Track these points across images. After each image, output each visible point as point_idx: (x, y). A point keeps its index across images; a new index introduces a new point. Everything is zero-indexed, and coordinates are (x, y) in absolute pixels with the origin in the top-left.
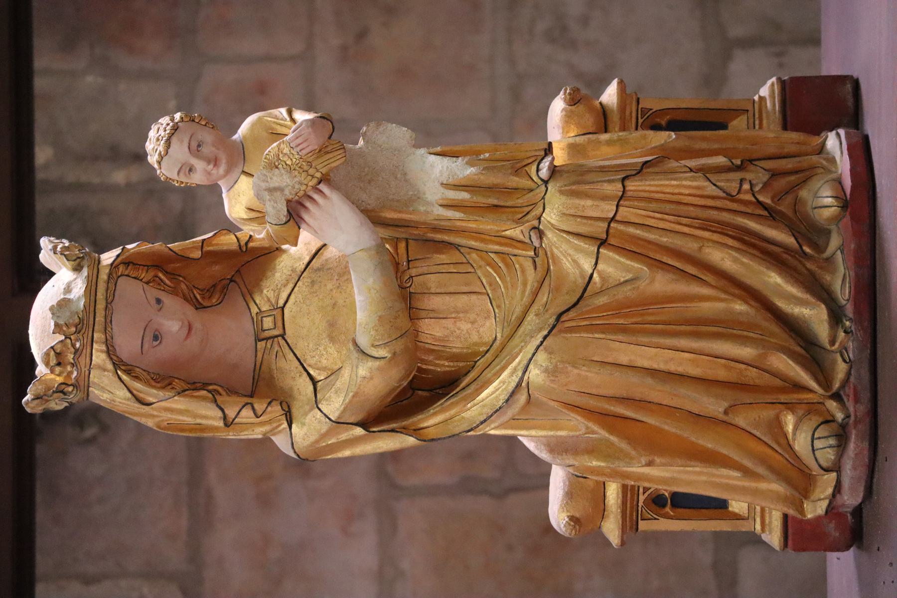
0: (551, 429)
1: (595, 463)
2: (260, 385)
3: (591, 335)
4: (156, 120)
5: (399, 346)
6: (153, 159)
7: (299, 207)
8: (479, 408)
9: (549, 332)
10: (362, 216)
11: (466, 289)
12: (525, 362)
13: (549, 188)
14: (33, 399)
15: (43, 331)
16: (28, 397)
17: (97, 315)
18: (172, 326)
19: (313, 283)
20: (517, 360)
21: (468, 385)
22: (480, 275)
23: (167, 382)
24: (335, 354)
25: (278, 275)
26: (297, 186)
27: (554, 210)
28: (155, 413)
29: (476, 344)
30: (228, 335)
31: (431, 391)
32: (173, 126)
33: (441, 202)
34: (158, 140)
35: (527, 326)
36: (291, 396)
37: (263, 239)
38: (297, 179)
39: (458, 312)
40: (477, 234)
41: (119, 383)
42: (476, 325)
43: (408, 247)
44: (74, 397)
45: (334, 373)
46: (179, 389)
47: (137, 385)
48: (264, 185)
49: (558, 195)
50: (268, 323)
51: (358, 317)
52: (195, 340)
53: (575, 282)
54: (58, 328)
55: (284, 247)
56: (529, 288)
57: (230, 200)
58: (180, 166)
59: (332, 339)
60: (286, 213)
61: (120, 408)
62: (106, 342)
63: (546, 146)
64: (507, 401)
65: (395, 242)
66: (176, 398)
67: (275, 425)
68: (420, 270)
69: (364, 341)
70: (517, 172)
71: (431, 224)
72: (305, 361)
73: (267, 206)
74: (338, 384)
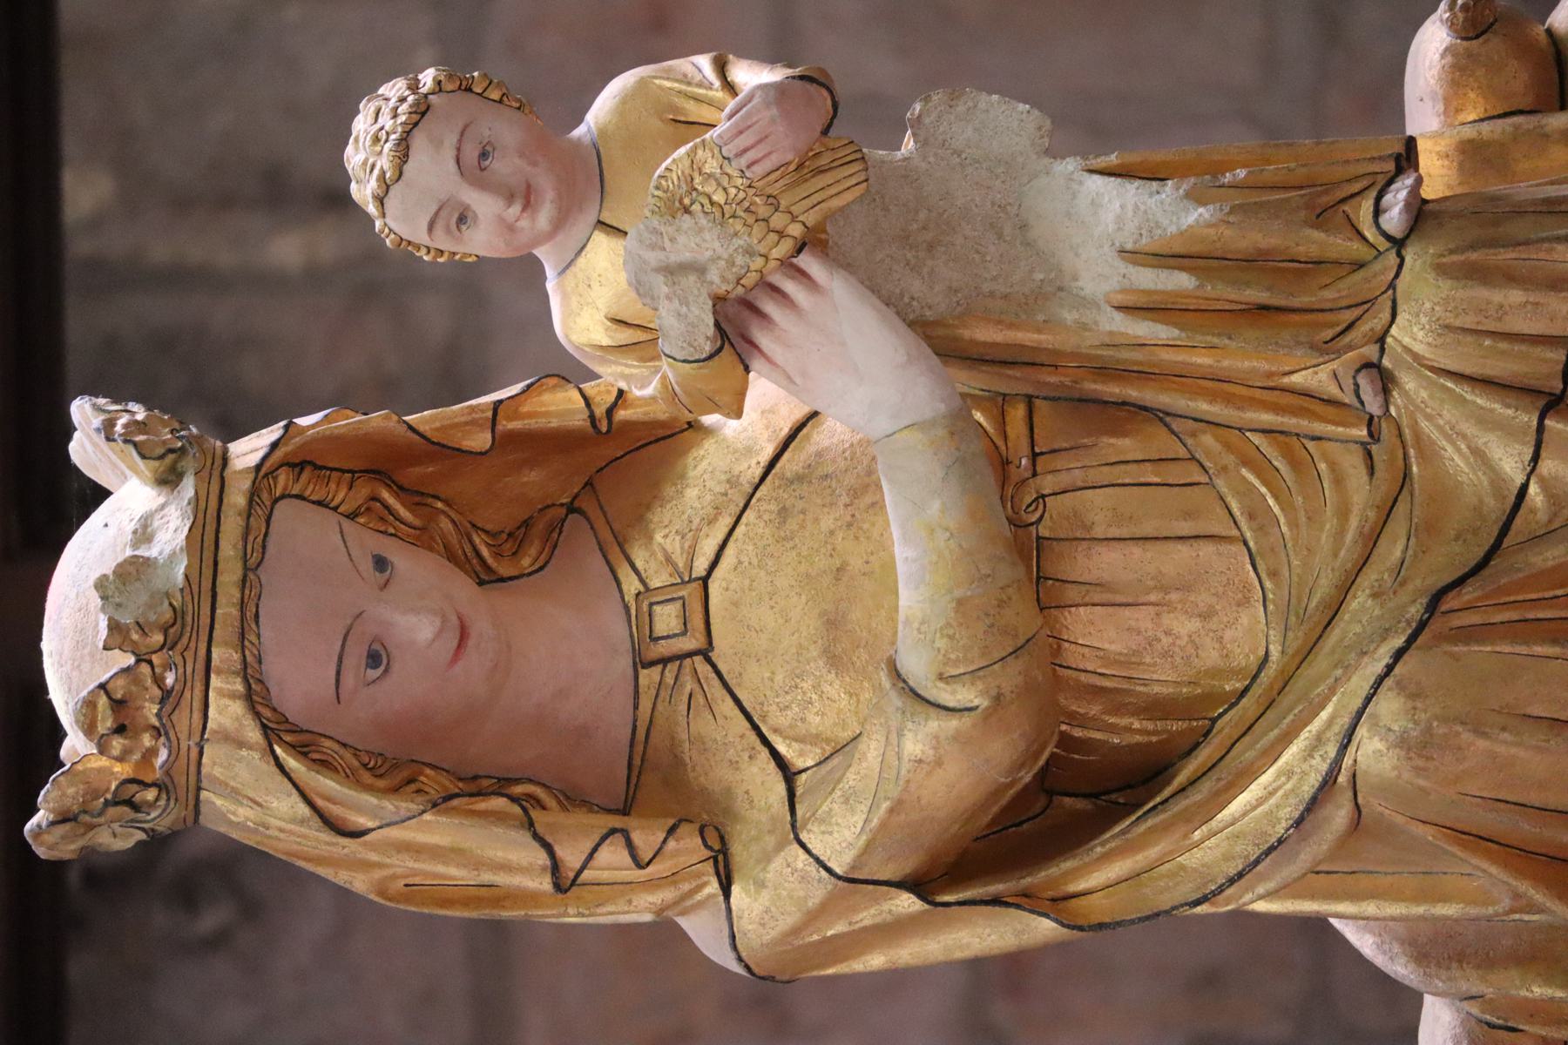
0: (1417, 899)
1: (1538, 991)
2: (649, 785)
3: (1523, 650)
4: (371, 89)
5: (1010, 678)
6: (363, 192)
7: (746, 313)
8: (1228, 838)
9: (1410, 641)
10: (910, 336)
11: (1185, 528)
12: (1345, 721)
13: (1408, 259)
14: (53, 824)
15: (78, 645)
16: (40, 818)
17: (221, 600)
18: (417, 630)
19: (784, 513)
20: (1324, 715)
21: (1193, 782)
22: (1224, 490)
23: (405, 774)
24: (844, 701)
25: (691, 493)
26: (740, 260)
27: (1420, 319)
28: (374, 857)
29: (1215, 673)
30: (562, 652)
31: (1096, 796)
32: (417, 104)
33: (1120, 299)
34: (376, 140)
35: (1349, 626)
36: (729, 812)
37: (653, 399)
38: (738, 242)
39: (1165, 590)
40: (1217, 384)
41: (280, 778)
42: (1214, 624)
43: (1035, 420)
44: (161, 818)
45: (841, 750)
46: (434, 795)
47: (326, 784)
48: (653, 258)
49: (1431, 276)
50: (666, 619)
51: (901, 603)
52: (476, 662)
53: (1478, 509)
54: (118, 635)
55: (709, 419)
56: (1354, 522)
57: (565, 297)
58: (434, 208)
59: (835, 661)
60: (711, 331)
61: (281, 846)
62: (245, 672)
63: (1399, 148)
64: (1299, 823)
65: (999, 404)
66: (427, 817)
67: (686, 887)
68: (1064, 480)
69: (917, 665)
70: (1322, 216)
71: (1089, 357)
72: (764, 717)
73: (663, 312)
74: (851, 778)
